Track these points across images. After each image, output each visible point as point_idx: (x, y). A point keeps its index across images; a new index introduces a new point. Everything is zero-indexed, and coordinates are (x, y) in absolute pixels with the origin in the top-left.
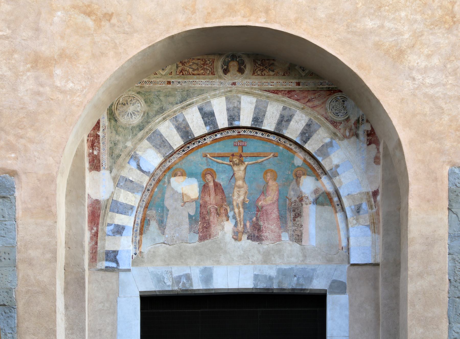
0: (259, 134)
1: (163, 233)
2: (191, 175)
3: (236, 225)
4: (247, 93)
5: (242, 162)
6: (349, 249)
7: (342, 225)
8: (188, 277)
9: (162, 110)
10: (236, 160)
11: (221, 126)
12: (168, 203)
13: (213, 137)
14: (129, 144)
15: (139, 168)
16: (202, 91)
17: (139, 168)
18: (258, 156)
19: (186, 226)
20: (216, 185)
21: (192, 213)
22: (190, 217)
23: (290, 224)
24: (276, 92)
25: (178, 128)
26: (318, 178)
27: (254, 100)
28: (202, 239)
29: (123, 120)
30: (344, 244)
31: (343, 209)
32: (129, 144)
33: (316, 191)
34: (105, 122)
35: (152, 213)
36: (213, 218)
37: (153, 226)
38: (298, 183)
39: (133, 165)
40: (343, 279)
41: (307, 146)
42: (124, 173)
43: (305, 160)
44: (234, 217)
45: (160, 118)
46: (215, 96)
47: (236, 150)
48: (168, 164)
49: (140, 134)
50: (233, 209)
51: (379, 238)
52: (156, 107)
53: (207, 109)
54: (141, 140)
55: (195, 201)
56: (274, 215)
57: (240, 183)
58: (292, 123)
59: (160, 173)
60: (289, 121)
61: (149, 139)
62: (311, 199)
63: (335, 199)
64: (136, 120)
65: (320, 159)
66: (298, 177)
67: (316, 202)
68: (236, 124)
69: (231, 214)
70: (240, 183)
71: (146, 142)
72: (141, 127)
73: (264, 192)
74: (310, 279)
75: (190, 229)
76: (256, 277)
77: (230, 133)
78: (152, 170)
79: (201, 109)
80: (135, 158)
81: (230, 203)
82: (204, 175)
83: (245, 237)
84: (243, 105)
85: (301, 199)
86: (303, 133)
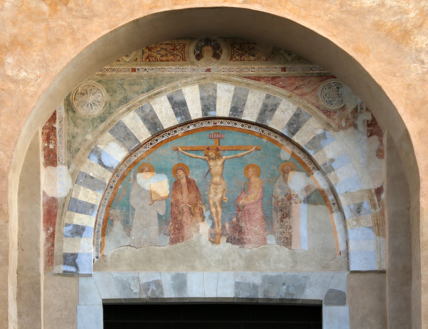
0: (239, 125)
1: (129, 235)
2: (160, 171)
3: (213, 226)
4: (224, 80)
5: (218, 156)
6: (348, 254)
7: (339, 227)
8: (158, 284)
9: (126, 100)
10: (212, 154)
11: (194, 117)
12: (134, 201)
13: (185, 129)
14: (89, 137)
15: (101, 162)
16: (171, 79)
17: (101, 162)
18: (238, 149)
19: (155, 226)
20: (190, 182)
21: (162, 213)
22: (160, 217)
23: (277, 225)
24: (257, 78)
25: (145, 120)
26: (309, 173)
27: (232, 88)
28: (173, 241)
29: (82, 111)
30: (342, 247)
31: (340, 209)
32: (89, 137)
33: (307, 189)
34: (61, 113)
35: (115, 212)
36: (186, 219)
37: (118, 227)
38: (285, 180)
39: (94, 160)
40: (342, 288)
41: (295, 138)
42: (84, 169)
43: (293, 154)
44: (211, 218)
45: (124, 108)
46: (186, 84)
47: (212, 143)
48: (134, 159)
49: (102, 126)
50: (209, 209)
51: (385, 242)
52: (119, 96)
53: (177, 98)
54: (103, 132)
55: (165, 199)
56: (258, 215)
57: (217, 179)
58: (277, 113)
59: (124, 168)
60: (273, 110)
61: (111, 132)
62: (302, 197)
63: (331, 197)
64: (97, 111)
65: (311, 152)
66: (285, 173)
67: (308, 200)
68: (211, 114)
69: (207, 214)
70: (217, 179)
71: (108, 135)
72: (102, 119)
73: (245, 190)
74: (302, 288)
75: (160, 230)
76: (237, 285)
77: (205, 124)
78: (115, 165)
79: (170, 99)
80: (97, 152)
81: (206, 202)
82: (175, 171)
83: (223, 240)
84: (219, 93)
85: (289, 197)
86: (290, 124)
